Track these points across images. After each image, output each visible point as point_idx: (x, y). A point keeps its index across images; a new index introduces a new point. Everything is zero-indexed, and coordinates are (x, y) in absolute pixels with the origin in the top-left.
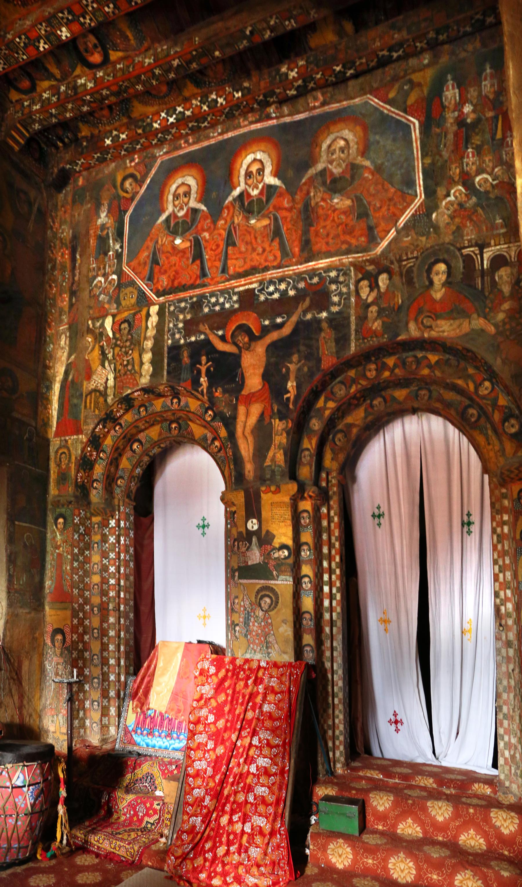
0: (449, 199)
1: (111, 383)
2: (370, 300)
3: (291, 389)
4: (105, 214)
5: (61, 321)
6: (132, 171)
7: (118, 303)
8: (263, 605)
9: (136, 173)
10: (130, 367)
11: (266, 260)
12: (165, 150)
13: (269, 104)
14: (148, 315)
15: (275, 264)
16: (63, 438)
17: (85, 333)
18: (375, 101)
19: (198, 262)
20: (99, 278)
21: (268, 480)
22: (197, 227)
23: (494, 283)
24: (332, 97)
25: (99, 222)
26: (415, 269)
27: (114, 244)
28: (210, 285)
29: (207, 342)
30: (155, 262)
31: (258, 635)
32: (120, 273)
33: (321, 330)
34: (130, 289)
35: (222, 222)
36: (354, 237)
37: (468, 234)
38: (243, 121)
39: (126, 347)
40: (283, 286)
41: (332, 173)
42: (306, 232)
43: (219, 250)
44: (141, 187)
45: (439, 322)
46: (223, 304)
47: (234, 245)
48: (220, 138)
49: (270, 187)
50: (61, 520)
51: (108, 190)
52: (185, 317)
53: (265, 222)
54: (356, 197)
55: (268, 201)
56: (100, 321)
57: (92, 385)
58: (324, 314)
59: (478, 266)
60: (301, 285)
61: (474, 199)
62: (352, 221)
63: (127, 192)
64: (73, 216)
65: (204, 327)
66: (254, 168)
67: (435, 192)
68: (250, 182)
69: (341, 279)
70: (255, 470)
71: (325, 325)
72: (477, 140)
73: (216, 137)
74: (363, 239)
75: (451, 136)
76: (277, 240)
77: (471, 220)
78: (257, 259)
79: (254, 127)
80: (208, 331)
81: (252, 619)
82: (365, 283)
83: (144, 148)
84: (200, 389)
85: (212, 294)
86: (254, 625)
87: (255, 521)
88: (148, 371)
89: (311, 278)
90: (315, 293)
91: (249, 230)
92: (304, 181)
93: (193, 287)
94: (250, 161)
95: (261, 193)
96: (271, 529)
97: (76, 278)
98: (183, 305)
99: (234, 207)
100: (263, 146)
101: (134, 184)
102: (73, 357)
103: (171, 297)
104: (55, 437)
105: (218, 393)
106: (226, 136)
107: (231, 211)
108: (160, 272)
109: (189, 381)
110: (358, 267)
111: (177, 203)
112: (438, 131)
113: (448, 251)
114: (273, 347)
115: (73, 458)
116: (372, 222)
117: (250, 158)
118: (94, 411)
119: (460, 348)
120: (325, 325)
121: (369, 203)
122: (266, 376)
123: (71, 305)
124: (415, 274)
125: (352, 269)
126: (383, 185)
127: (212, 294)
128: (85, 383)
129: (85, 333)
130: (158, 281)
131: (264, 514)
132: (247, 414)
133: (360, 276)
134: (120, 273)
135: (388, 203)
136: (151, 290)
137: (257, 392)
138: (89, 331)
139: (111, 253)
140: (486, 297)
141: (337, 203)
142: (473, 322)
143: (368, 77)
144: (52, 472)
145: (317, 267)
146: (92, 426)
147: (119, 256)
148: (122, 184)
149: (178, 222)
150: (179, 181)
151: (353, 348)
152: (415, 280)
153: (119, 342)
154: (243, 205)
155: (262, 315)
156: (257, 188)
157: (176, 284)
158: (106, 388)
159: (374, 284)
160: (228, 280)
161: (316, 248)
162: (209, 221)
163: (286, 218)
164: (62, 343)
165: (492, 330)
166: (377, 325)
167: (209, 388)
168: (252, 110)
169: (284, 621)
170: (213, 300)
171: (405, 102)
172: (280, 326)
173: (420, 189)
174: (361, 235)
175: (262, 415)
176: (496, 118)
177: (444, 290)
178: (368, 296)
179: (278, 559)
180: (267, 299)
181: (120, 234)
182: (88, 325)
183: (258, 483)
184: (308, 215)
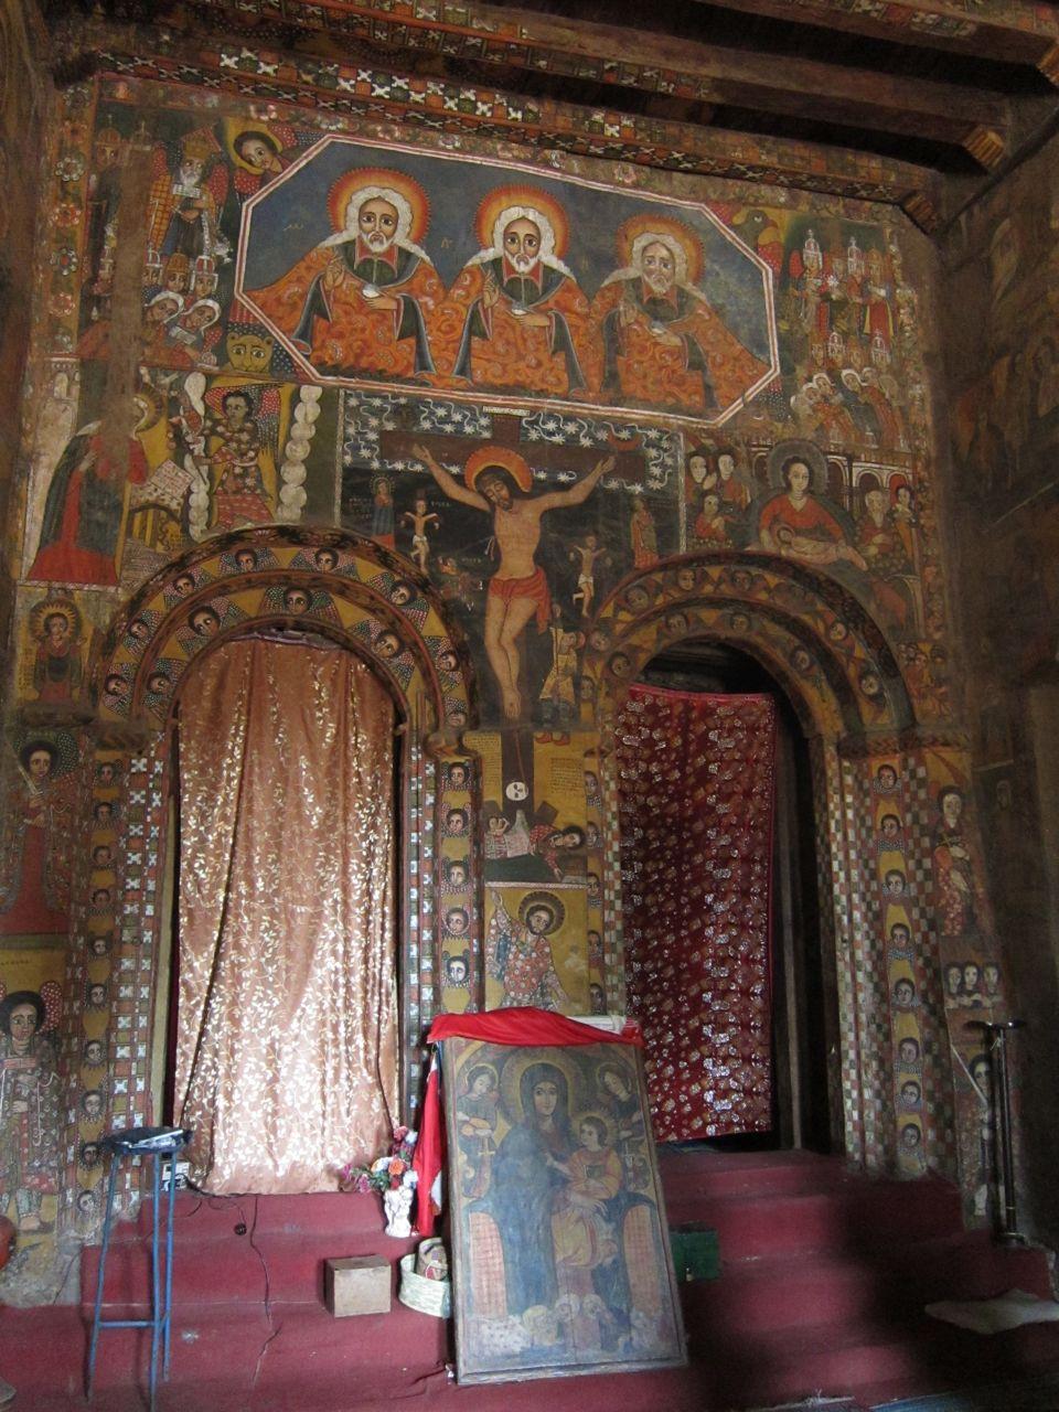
0: (810, 385)
1: (200, 498)
2: (707, 486)
3: (584, 587)
4: (194, 180)
5: (57, 346)
6: (263, 129)
7: (223, 359)
8: (534, 921)
9: (272, 136)
10: (250, 482)
11: (543, 380)
12: (340, 126)
13: (553, 146)
14: (296, 399)
15: (559, 391)
16: (57, 585)
17: (130, 389)
18: (713, 217)
19: (412, 341)
20: (171, 295)
21: (547, 721)
22: (410, 282)
23: (864, 509)
24: (649, 180)
25: (177, 190)
26: (768, 461)
27: (213, 244)
28: (434, 386)
29: (426, 480)
30: (317, 308)
31: (524, 974)
32: (228, 304)
33: (633, 510)
34: (248, 339)
35: (460, 292)
36: (685, 391)
37: (833, 438)
38: (503, 149)
39: (239, 442)
40: (571, 428)
41: (650, 291)
42: (610, 361)
43: (455, 336)
44: (284, 168)
45: (799, 539)
46: (460, 424)
47: (484, 336)
48: (459, 157)
49: (549, 270)
50: (42, 755)
51: (204, 140)
52: (381, 424)
53: (544, 322)
54: (687, 336)
55: (546, 290)
56: (174, 376)
57: (148, 494)
58: (638, 488)
59: (846, 482)
60: (602, 435)
61: (839, 398)
62: (681, 367)
63: (250, 162)
64: (96, 152)
65: (424, 453)
66: (522, 231)
67: (794, 370)
68: (514, 247)
69: (665, 445)
70: (523, 703)
71: (638, 504)
72: (843, 324)
73: (448, 149)
74: (697, 398)
75: (812, 307)
76: (563, 355)
77: (838, 422)
78: (522, 372)
79: (522, 167)
80: (430, 461)
81: (513, 949)
82: (699, 461)
83: (298, 101)
84: (413, 554)
85: (439, 403)
86: (516, 958)
87: (521, 785)
88: (298, 494)
89: (617, 430)
90: (622, 453)
91: (509, 323)
92: (606, 282)
93: (398, 378)
94: (515, 217)
95: (534, 271)
96: (549, 800)
97: (105, 273)
98: (377, 402)
99: (483, 277)
100: (540, 203)
101: (267, 155)
102: (92, 427)
103: (353, 382)
104: (28, 579)
105: (449, 568)
106: (470, 159)
107: (479, 281)
108: (329, 327)
109: (392, 537)
110: (692, 436)
111: (368, 226)
112: (797, 293)
113: (809, 450)
114: (552, 517)
115: (88, 631)
116: (712, 382)
117: (515, 212)
118: (153, 546)
119: (822, 578)
120: (638, 504)
121: (707, 353)
122: (540, 557)
123: (86, 323)
124: (768, 468)
125: (681, 435)
126: (725, 336)
127: (439, 403)
128: (129, 487)
129: (130, 389)
130: (323, 346)
131: (537, 773)
132: (506, 613)
133: (693, 449)
134: (228, 304)
135: (732, 362)
136: (307, 357)
137: (523, 580)
138: (139, 386)
139: (204, 257)
140: (855, 523)
141: (659, 335)
142: (842, 550)
143: (704, 180)
144: (20, 651)
145: (628, 416)
146: (145, 575)
147: (225, 271)
148: (239, 144)
149: (370, 261)
150: (374, 192)
151: (683, 549)
152: (768, 476)
153: (220, 429)
154: (499, 278)
155: (535, 461)
156: (527, 263)
157: (364, 362)
158: (186, 507)
159: (712, 467)
160: (472, 390)
161: (628, 388)
162: (434, 281)
163: (578, 328)
164: (60, 388)
165: (864, 565)
166: (717, 523)
167: (432, 553)
168: (524, 142)
169: (574, 949)
170: (441, 412)
171: (756, 238)
172: (565, 487)
173: (775, 359)
174: (695, 393)
175: (533, 617)
176: (864, 306)
177: (805, 499)
178: (704, 479)
179: (563, 848)
180: (541, 439)
181: (229, 230)
182: (139, 378)
183: (530, 725)
184: (613, 333)
